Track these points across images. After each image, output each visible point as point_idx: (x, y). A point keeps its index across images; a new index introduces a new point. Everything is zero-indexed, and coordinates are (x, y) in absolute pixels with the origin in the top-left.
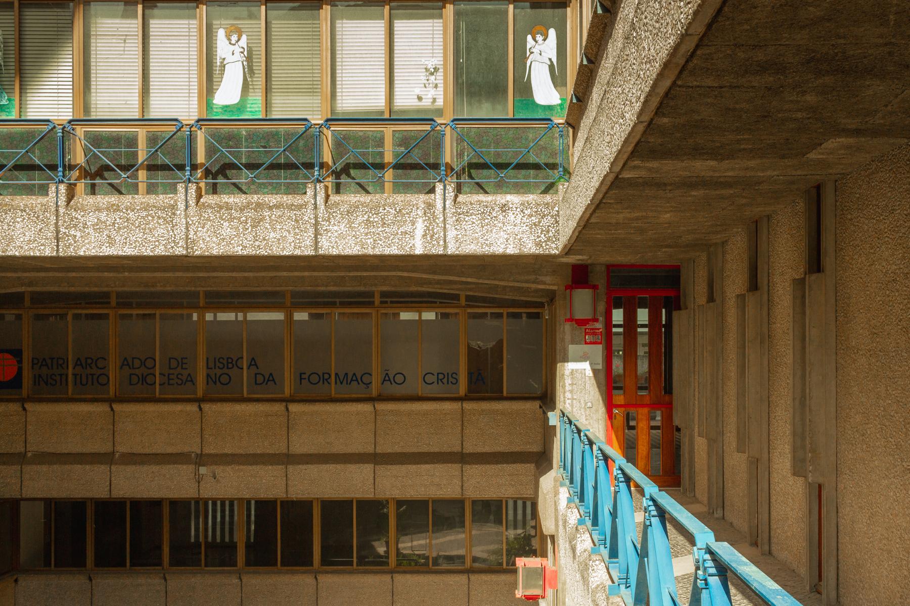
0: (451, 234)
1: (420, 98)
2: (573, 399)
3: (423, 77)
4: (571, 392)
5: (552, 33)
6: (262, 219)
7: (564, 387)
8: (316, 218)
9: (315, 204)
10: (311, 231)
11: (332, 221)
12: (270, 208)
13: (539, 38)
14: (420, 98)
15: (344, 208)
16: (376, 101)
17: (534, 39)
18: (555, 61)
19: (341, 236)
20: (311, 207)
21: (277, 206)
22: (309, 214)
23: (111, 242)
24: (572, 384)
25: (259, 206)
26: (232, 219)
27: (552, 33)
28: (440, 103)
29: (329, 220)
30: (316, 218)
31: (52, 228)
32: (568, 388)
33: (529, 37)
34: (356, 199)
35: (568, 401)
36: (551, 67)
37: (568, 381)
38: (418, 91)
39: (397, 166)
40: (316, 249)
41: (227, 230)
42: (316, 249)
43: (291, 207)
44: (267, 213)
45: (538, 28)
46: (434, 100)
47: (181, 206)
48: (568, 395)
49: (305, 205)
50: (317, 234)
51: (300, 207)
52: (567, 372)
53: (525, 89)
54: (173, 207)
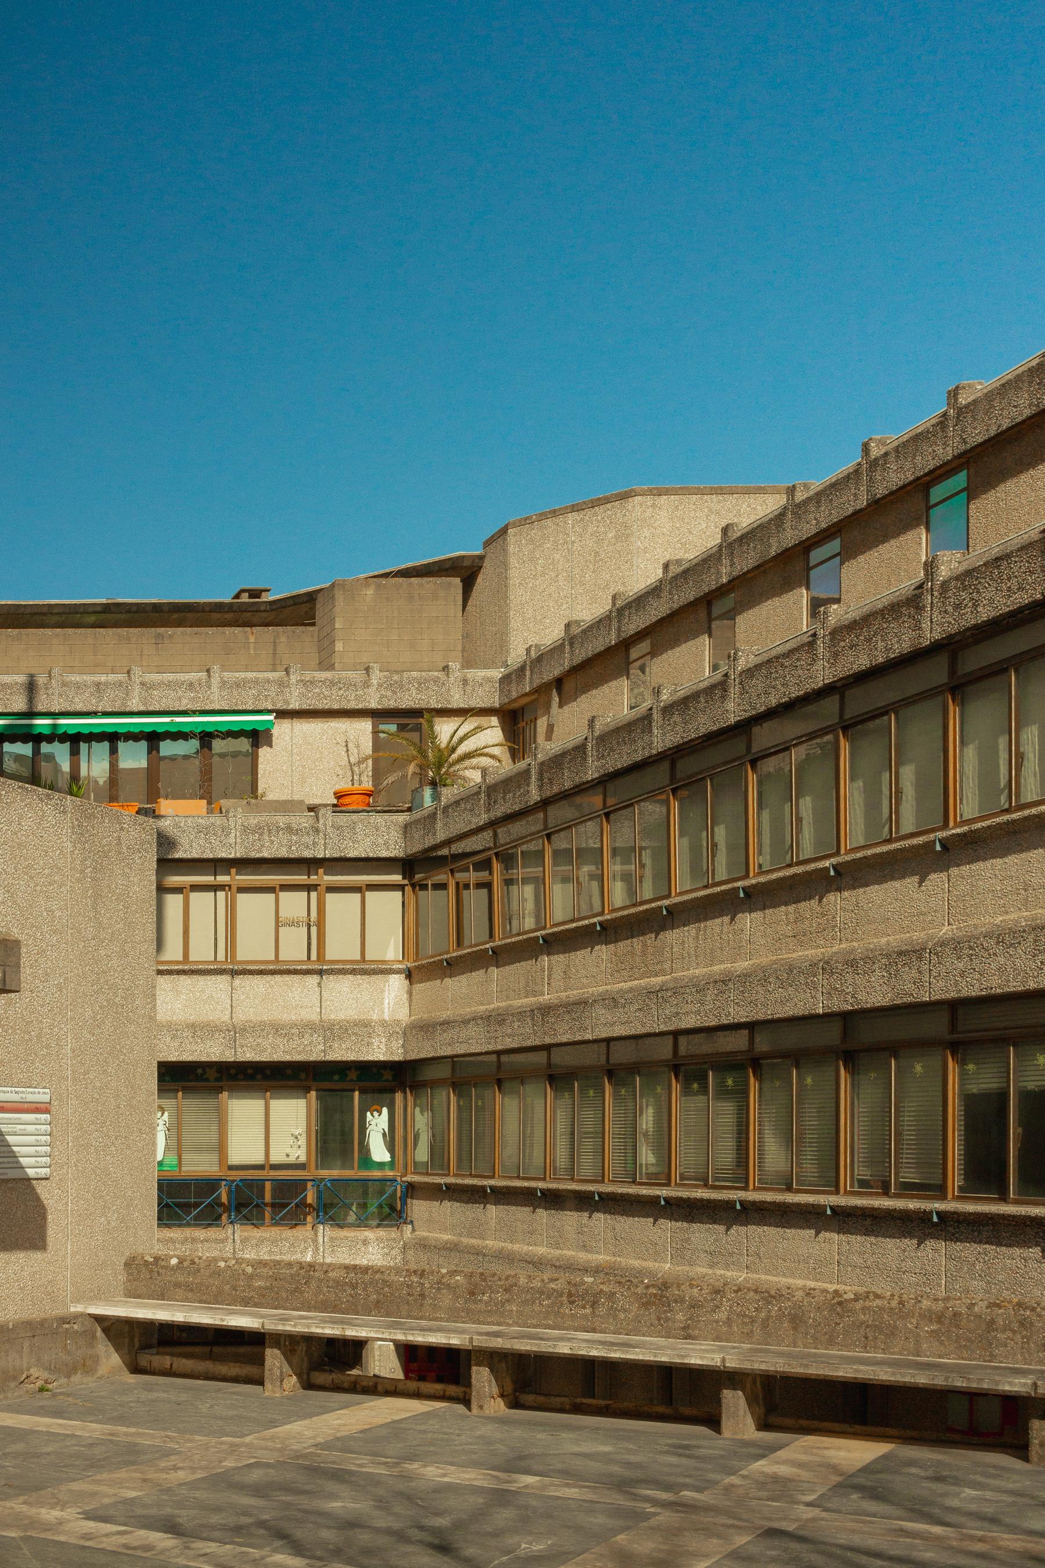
1: (288, 1155)
2: (380, 1366)
3: (291, 1141)
4: (379, 1361)
5: (385, 1110)
7: (374, 1357)
9: (234, 1239)
11: (246, 1251)
13: (376, 1114)
14: (288, 1155)
15: (254, 1242)
16: (258, 1158)
17: (372, 1115)
18: (386, 1130)
20: (231, 1241)
24: (380, 1355)
27: (385, 1110)
28: (303, 1159)
29: (243, 1250)
30: (234, 1249)
32: (377, 1358)
33: (369, 1114)
34: (259, 1234)
35: (377, 1368)
36: (384, 1135)
37: (377, 1353)
38: (288, 1150)
39: (273, 1205)
45: (375, 1107)
46: (298, 1157)
48: (377, 1363)
49: (227, 1239)
51: (224, 1241)
52: (376, 1347)
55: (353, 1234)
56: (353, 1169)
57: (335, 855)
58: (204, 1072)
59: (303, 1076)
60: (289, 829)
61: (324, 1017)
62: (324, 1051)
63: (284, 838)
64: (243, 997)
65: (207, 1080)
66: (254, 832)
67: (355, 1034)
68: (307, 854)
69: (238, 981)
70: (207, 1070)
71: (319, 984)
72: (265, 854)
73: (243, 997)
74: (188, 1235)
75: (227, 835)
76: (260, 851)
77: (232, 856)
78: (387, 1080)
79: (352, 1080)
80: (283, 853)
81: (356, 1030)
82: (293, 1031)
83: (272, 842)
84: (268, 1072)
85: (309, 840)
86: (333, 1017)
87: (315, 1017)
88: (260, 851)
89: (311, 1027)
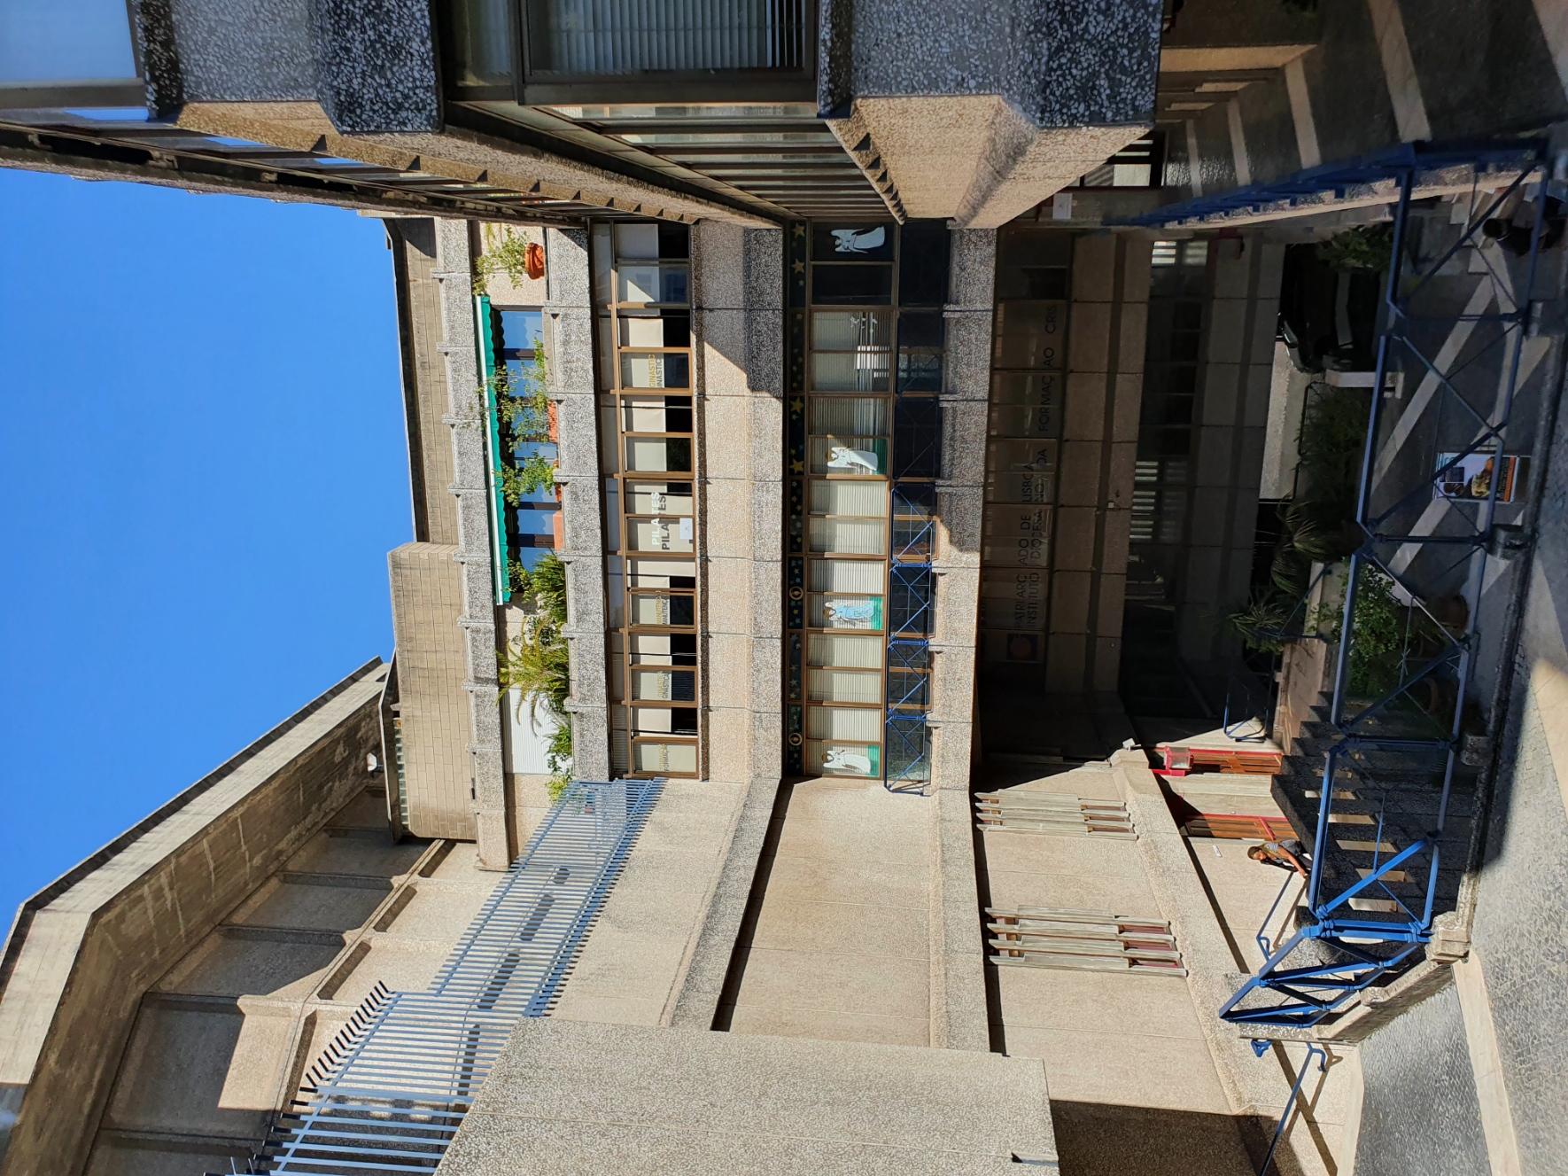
0: (979, 306)
5: (835, 233)
6: (962, 436)
8: (963, 400)
10: (971, 403)
12: (955, 431)
13: (838, 242)
19: (976, 383)
20: (955, 404)
21: (953, 426)
22: (961, 406)
23: (971, 535)
25: (952, 439)
26: (961, 457)
27: (835, 233)
29: (965, 392)
30: (963, 400)
31: (961, 571)
33: (837, 249)
36: (858, 233)
40: (984, 400)
41: (968, 461)
42: (984, 400)
43: (954, 419)
44: (958, 434)
47: (950, 490)
50: (974, 400)
53: (872, 253)
54: (950, 495)
55: (954, 279)
56: (890, 267)
57: (588, 298)
58: (795, 412)
59: (799, 316)
60: (566, 343)
61: (742, 306)
62: (774, 310)
63: (574, 348)
64: (723, 385)
65: (803, 410)
66: (570, 377)
67: (757, 278)
68: (588, 325)
69: (709, 391)
70: (793, 409)
71: (711, 310)
72: (590, 366)
73: (723, 385)
74: (948, 442)
75: (575, 403)
76: (586, 371)
77: (593, 397)
78: (805, 231)
79: (804, 267)
80: (588, 349)
81: (753, 278)
82: (754, 342)
83: (578, 359)
84: (796, 351)
85: (574, 325)
86: (741, 298)
87: (742, 315)
88: (586, 371)
89: (749, 323)
